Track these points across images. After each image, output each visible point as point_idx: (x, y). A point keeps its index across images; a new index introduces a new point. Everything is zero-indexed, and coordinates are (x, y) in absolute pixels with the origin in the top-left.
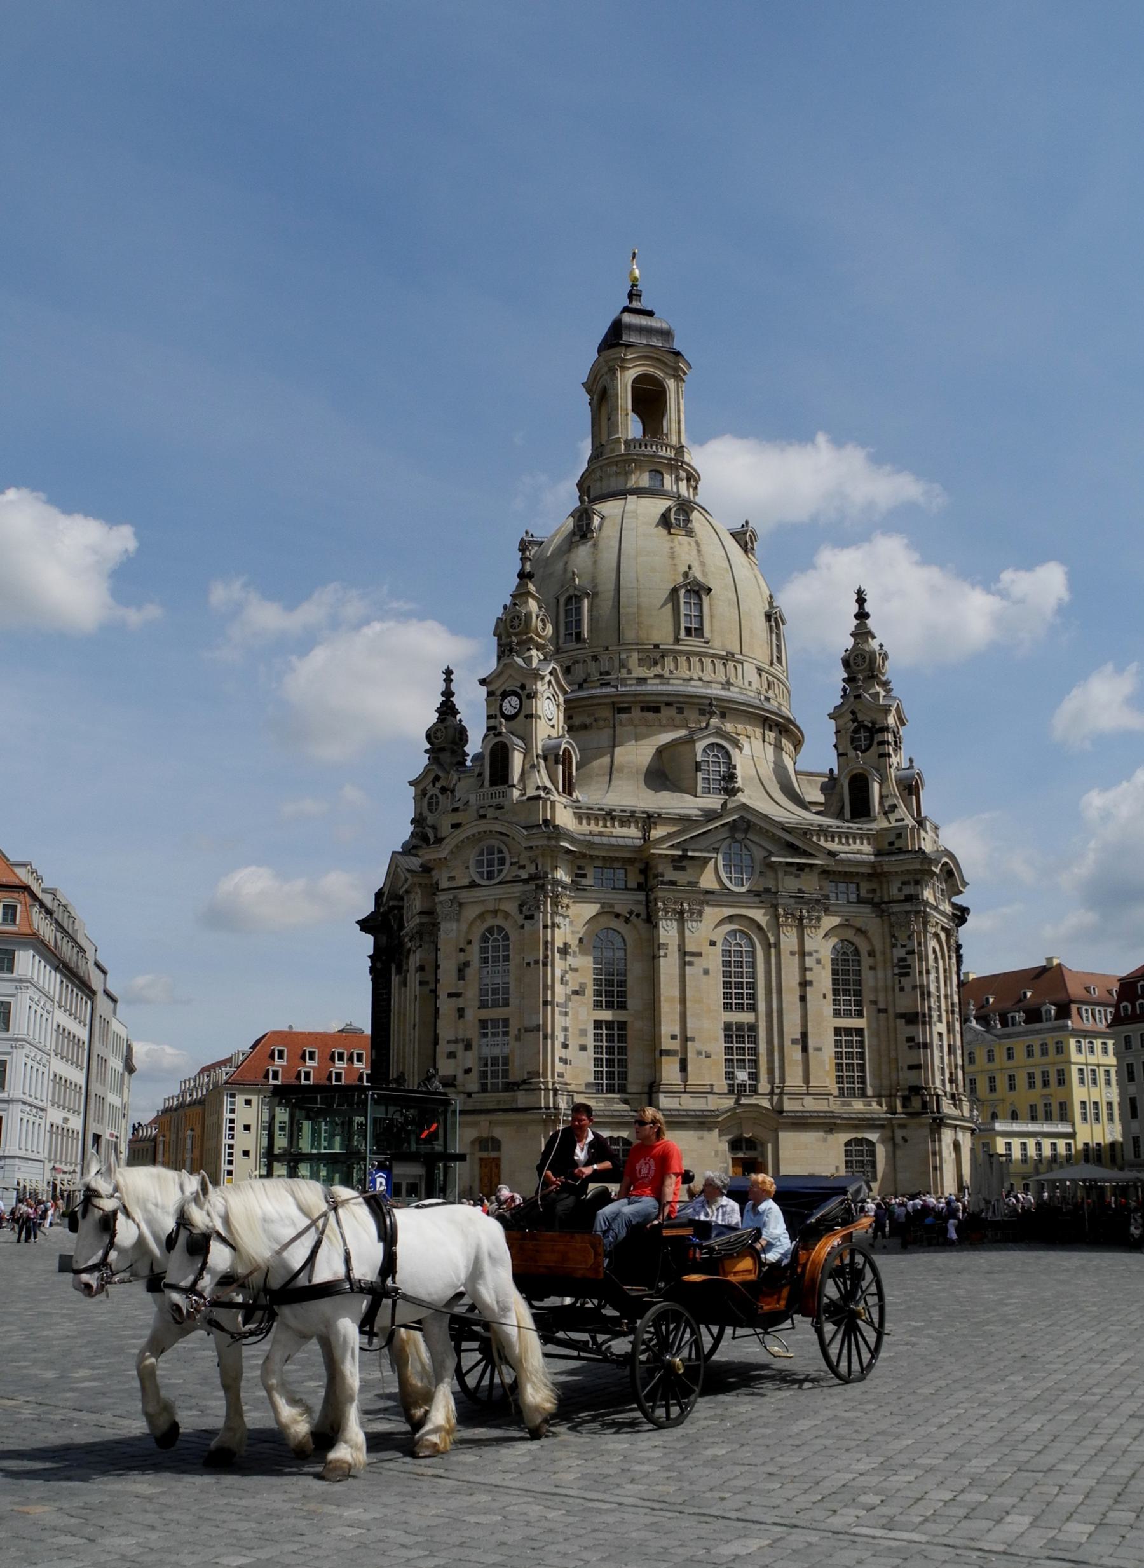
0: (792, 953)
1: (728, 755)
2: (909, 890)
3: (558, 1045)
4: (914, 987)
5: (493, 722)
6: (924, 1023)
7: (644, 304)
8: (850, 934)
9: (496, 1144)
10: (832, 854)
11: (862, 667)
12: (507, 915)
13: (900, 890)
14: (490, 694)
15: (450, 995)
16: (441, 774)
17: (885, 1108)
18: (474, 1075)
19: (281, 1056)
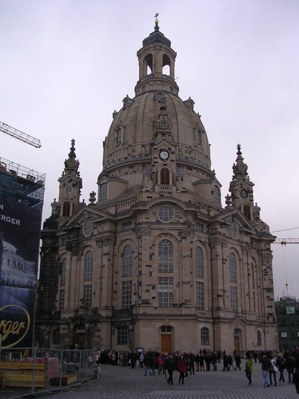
0: (246, 263)
2: (267, 246)
4: (269, 279)
10: (256, 230)
12: (172, 235)
13: (265, 246)
15: (147, 266)
18: (157, 299)
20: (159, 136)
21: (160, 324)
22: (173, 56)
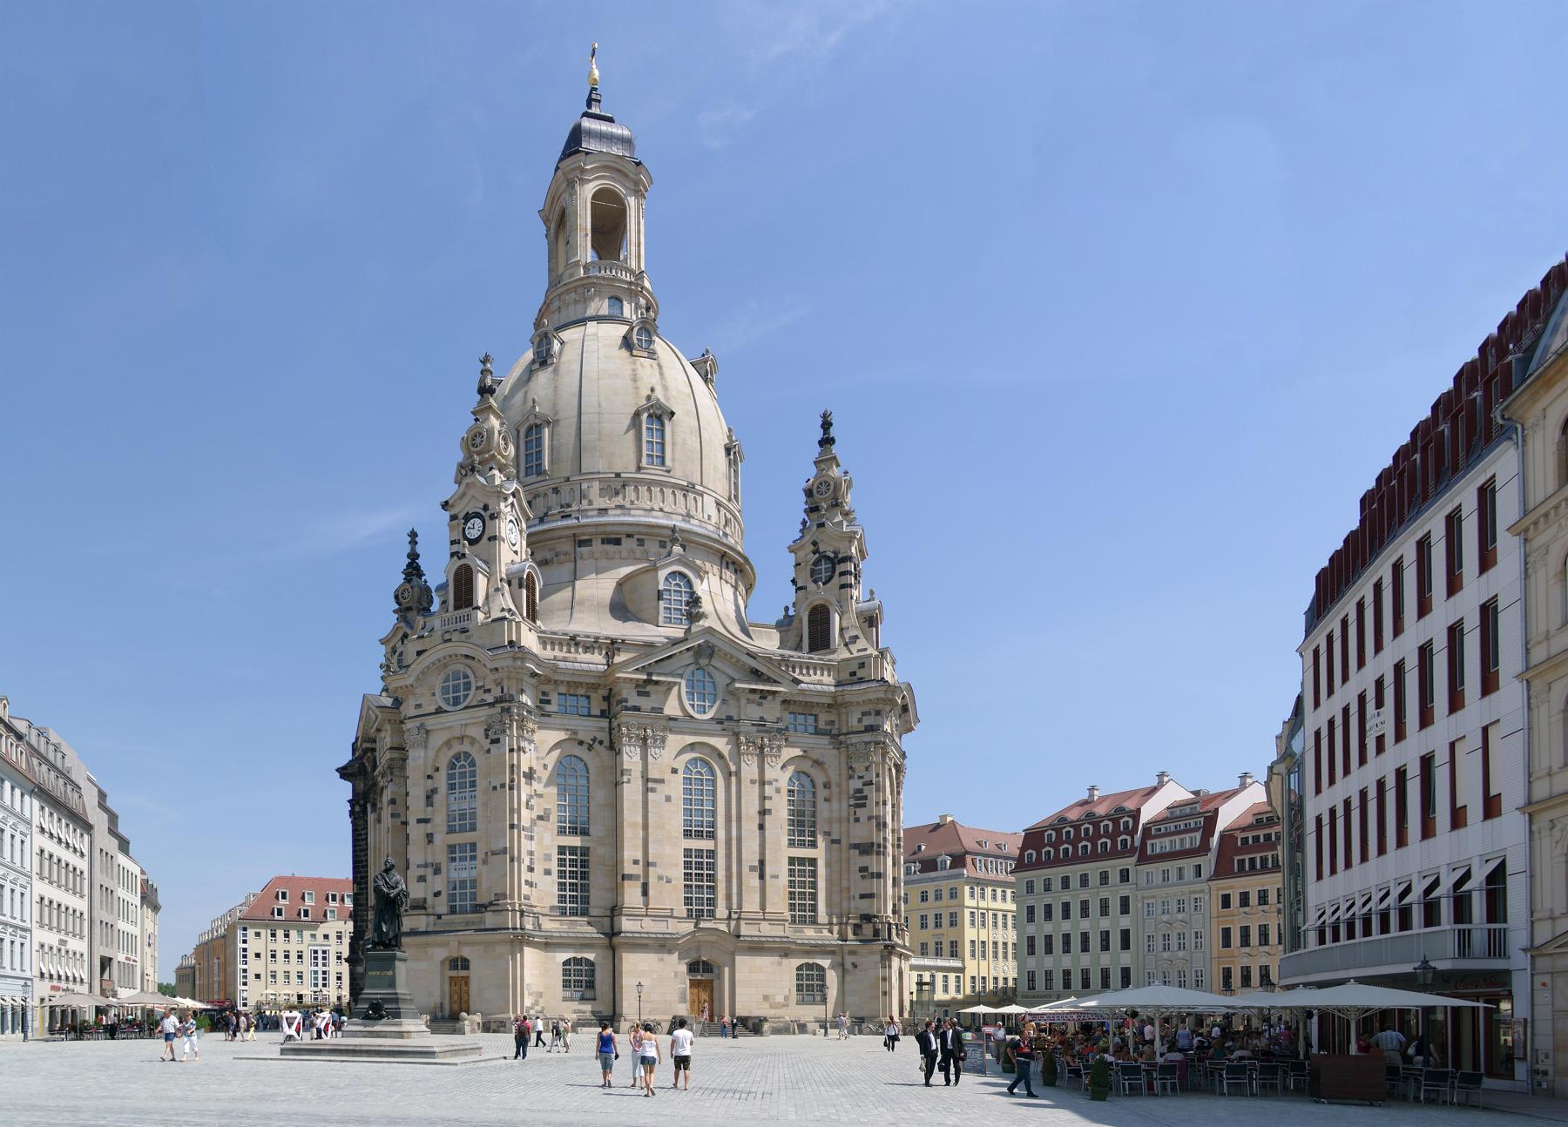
0: (753, 782)
1: (689, 584)
3: (524, 868)
4: (870, 818)
5: (455, 548)
6: (878, 853)
8: (806, 766)
11: (823, 499)
12: (473, 741)
14: (453, 518)
17: (836, 935)
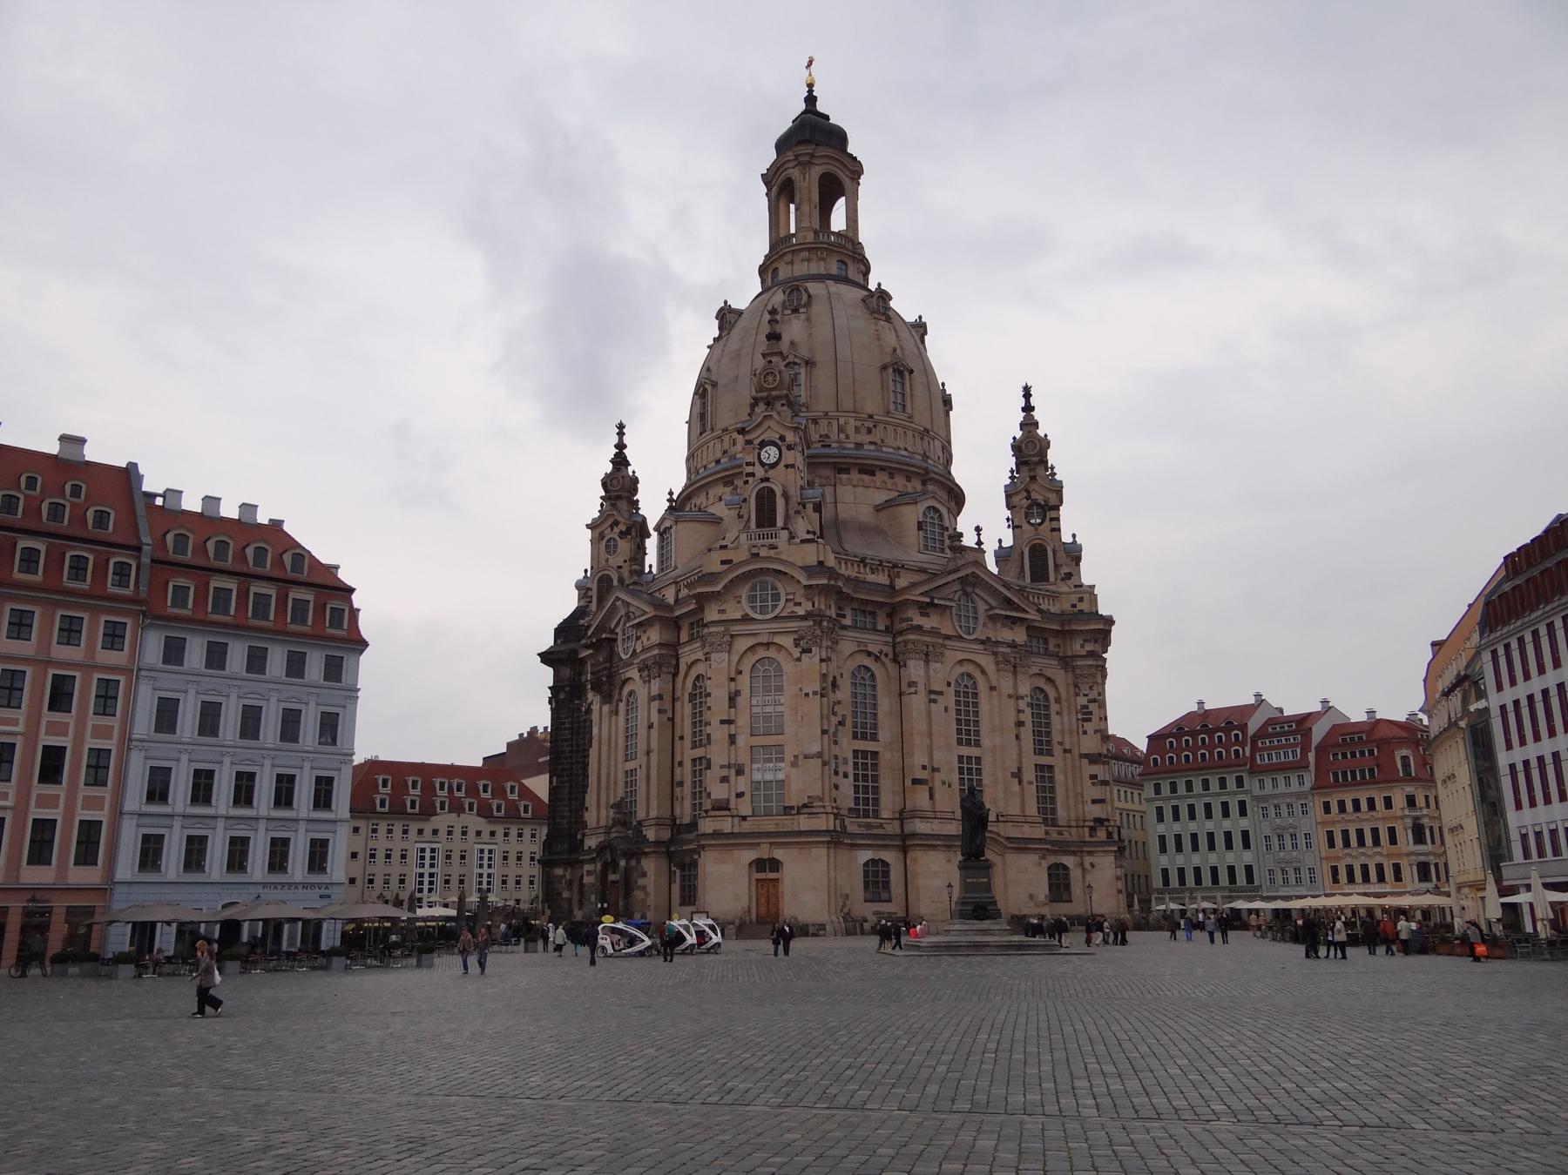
1: (941, 517)
2: (1089, 647)
4: (1096, 732)
7: (820, 107)
8: (1041, 683)
9: (775, 865)
10: (1040, 611)
11: (1030, 451)
15: (723, 722)
16: (620, 519)
18: (747, 798)
19: (385, 785)
20: (761, 408)
21: (752, 855)
22: (853, 172)
